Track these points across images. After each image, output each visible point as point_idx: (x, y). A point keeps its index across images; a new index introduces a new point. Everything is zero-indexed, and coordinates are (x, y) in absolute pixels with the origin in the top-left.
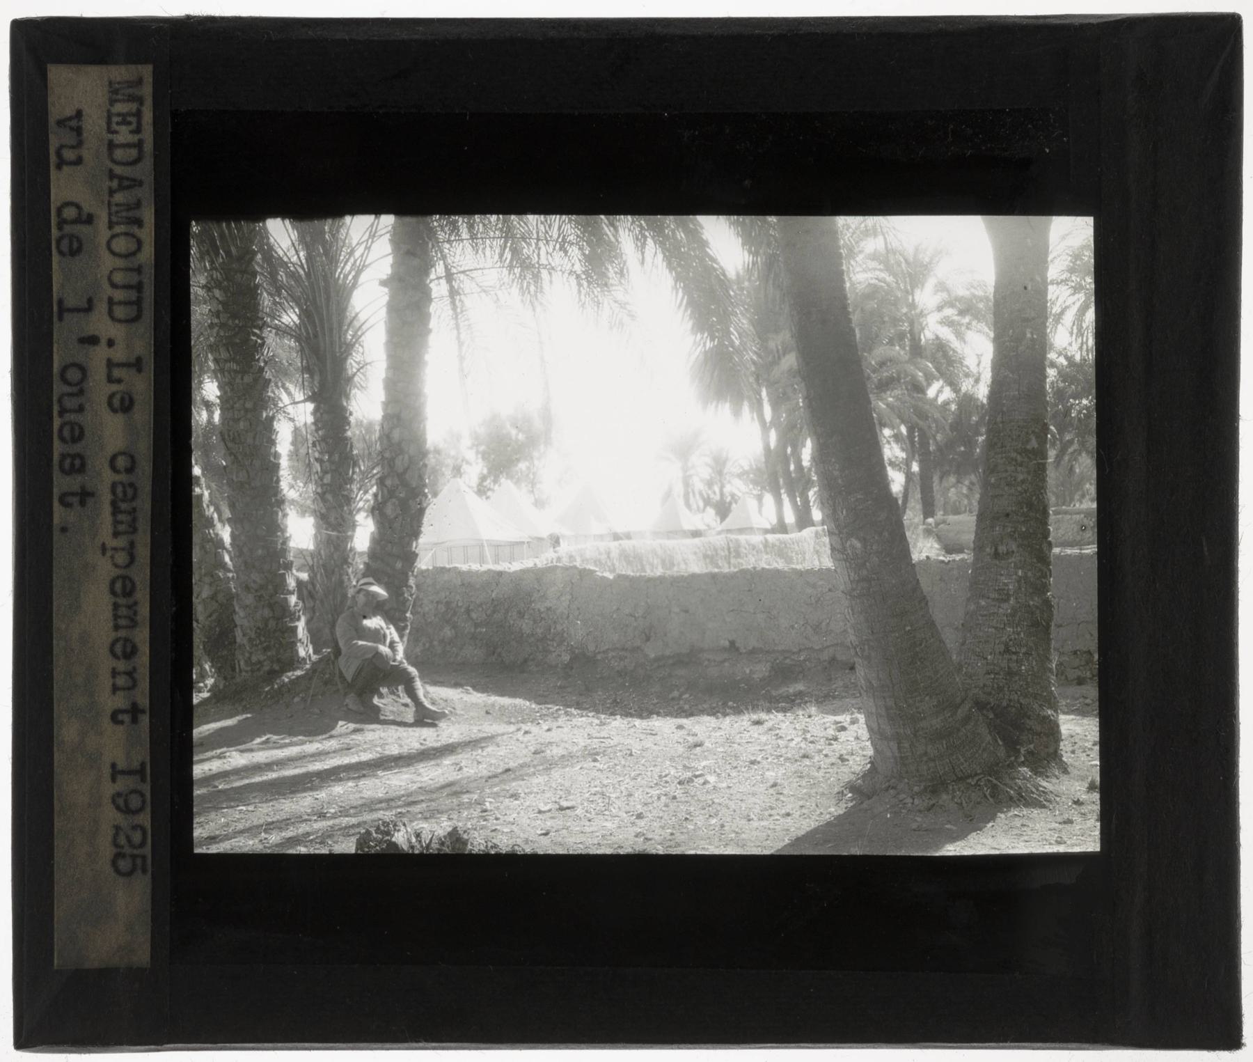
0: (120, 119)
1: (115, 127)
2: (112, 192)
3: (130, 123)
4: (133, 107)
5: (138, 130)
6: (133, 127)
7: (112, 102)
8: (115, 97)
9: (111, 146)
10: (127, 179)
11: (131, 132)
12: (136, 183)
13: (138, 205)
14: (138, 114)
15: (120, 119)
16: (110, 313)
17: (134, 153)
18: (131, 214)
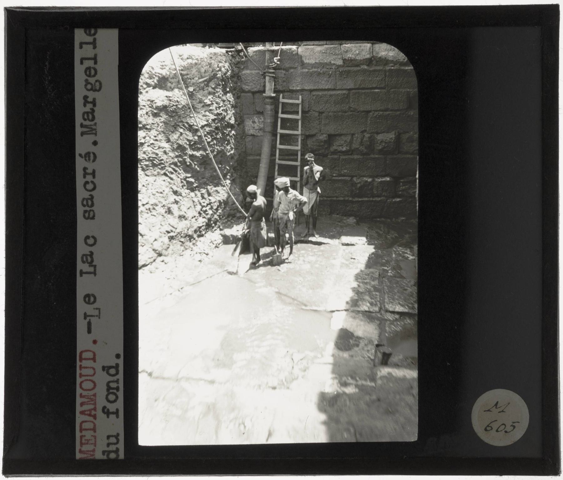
0: (91, 442)
1: (93, 438)
2: (95, 409)
3: (85, 440)
4: (84, 448)
5: (81, 437)
6: (83, 439)
7: (94, 451)
8: (92, 453)
9: (94, 430)
10: (87, 415)
11: (85, 436)
12: (82, 413)
13: (82, 404)
14: (82, 444)
15: (91, 442)
16: (94, 354)
17: (85, 426)
18: (86, 400)
